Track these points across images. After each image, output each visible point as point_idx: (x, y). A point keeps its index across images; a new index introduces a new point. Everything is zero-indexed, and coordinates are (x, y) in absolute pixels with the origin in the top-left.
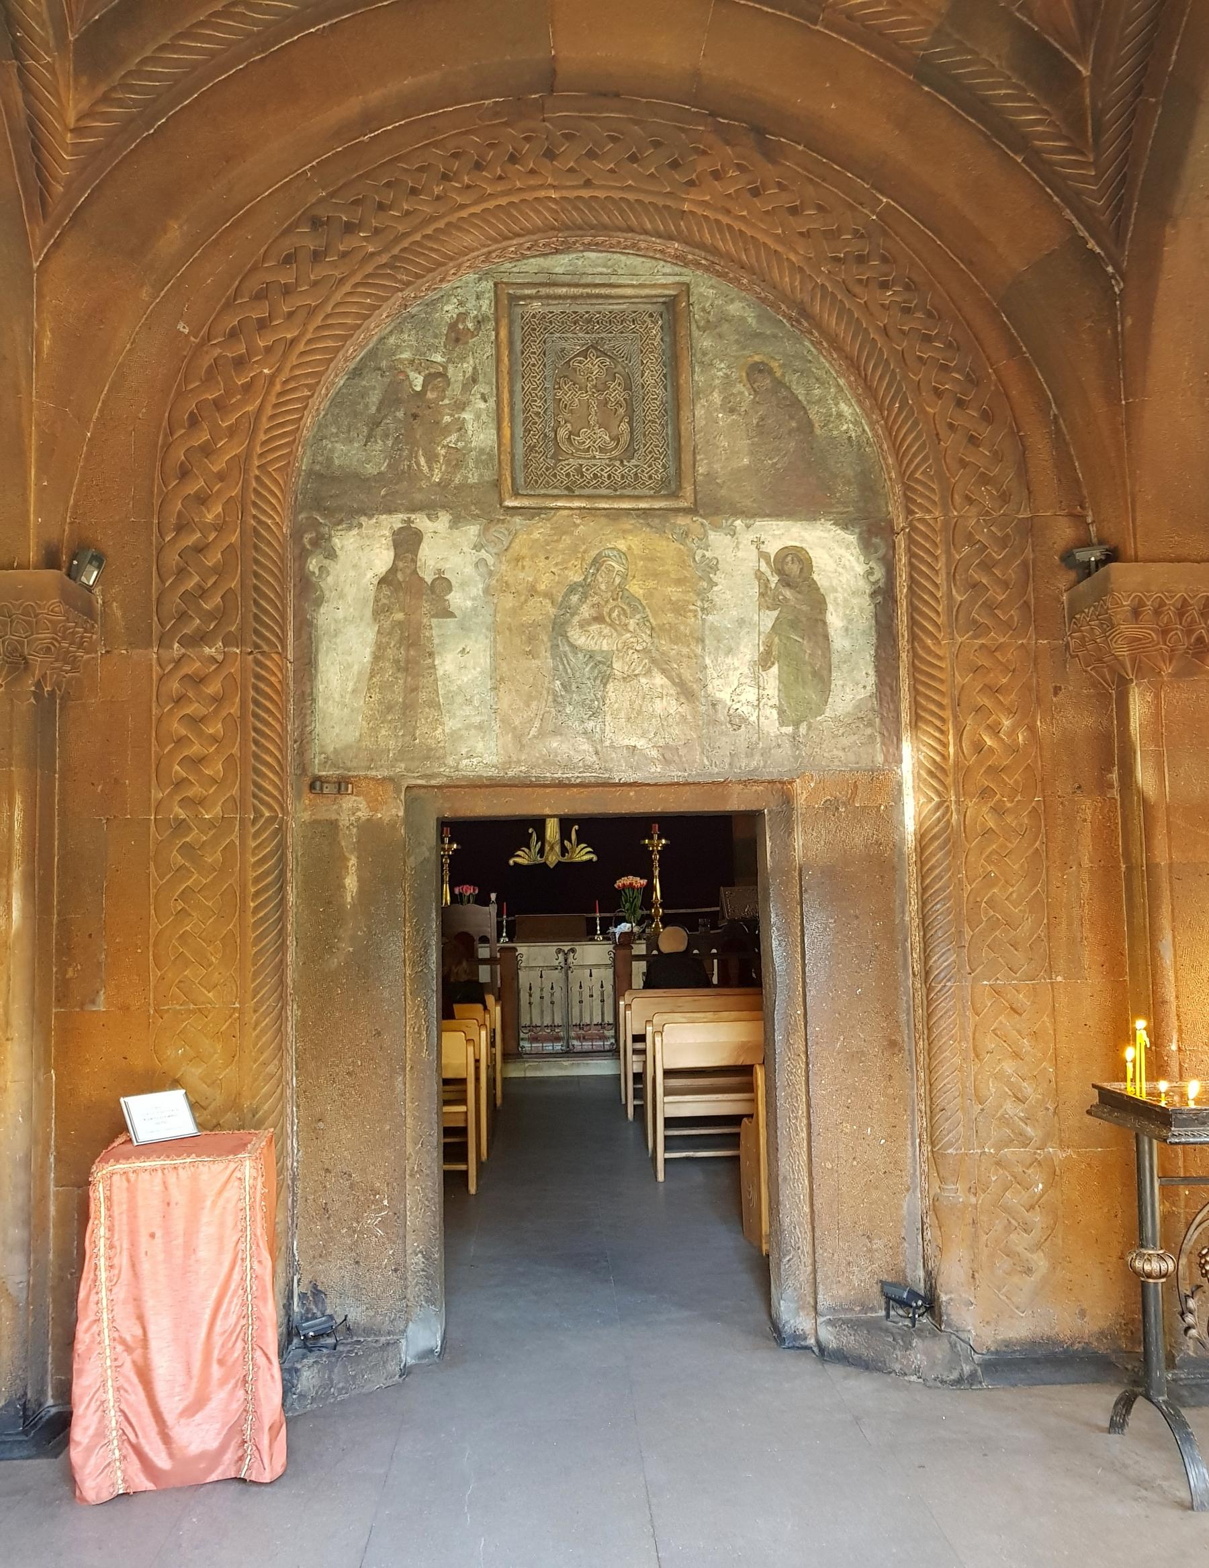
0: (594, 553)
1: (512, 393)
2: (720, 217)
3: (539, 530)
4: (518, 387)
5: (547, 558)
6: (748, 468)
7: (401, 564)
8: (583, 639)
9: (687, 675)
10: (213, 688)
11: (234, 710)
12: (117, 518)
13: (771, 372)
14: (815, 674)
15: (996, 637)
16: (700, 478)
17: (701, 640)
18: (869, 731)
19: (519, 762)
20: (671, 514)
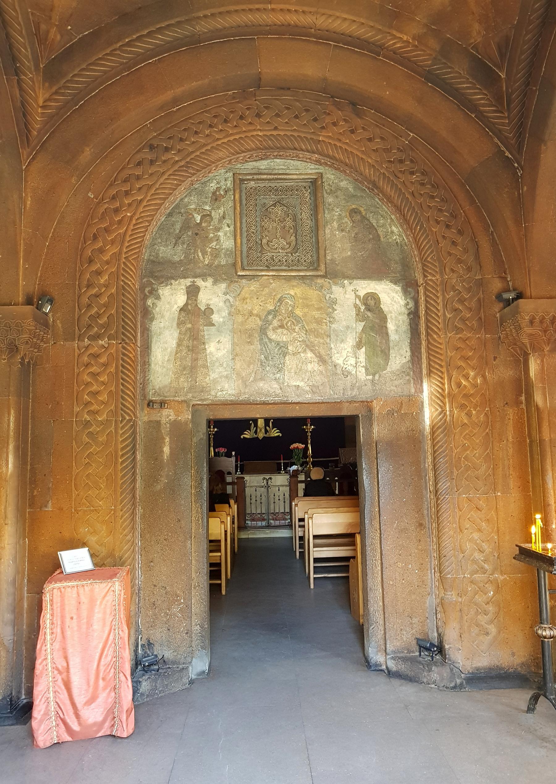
0: (279, 296)
1: (241, 223)
2: (336, 143)
3: (254, 286)
4: (244, 221)
5: (258, 298)
6: (350, 256)
7: (190, 302)
8: (274, 336)
9: (323, 352)
10: (103, 360)
11: (113, 370)
12: (60, 282)
13: (360, 212)
14: (382, 351)
15: (466, 334)
18: (408, 378)
19: (245, 393)
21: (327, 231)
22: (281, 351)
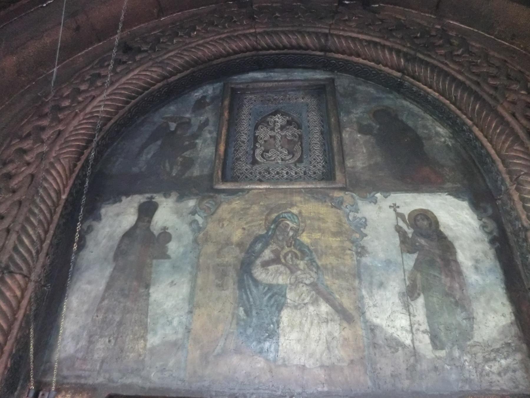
0: (274, 216)
3: (237, 204)
8: (263, 275)
17: (358, 275)
20: (328, 191)
22: (273, 300)
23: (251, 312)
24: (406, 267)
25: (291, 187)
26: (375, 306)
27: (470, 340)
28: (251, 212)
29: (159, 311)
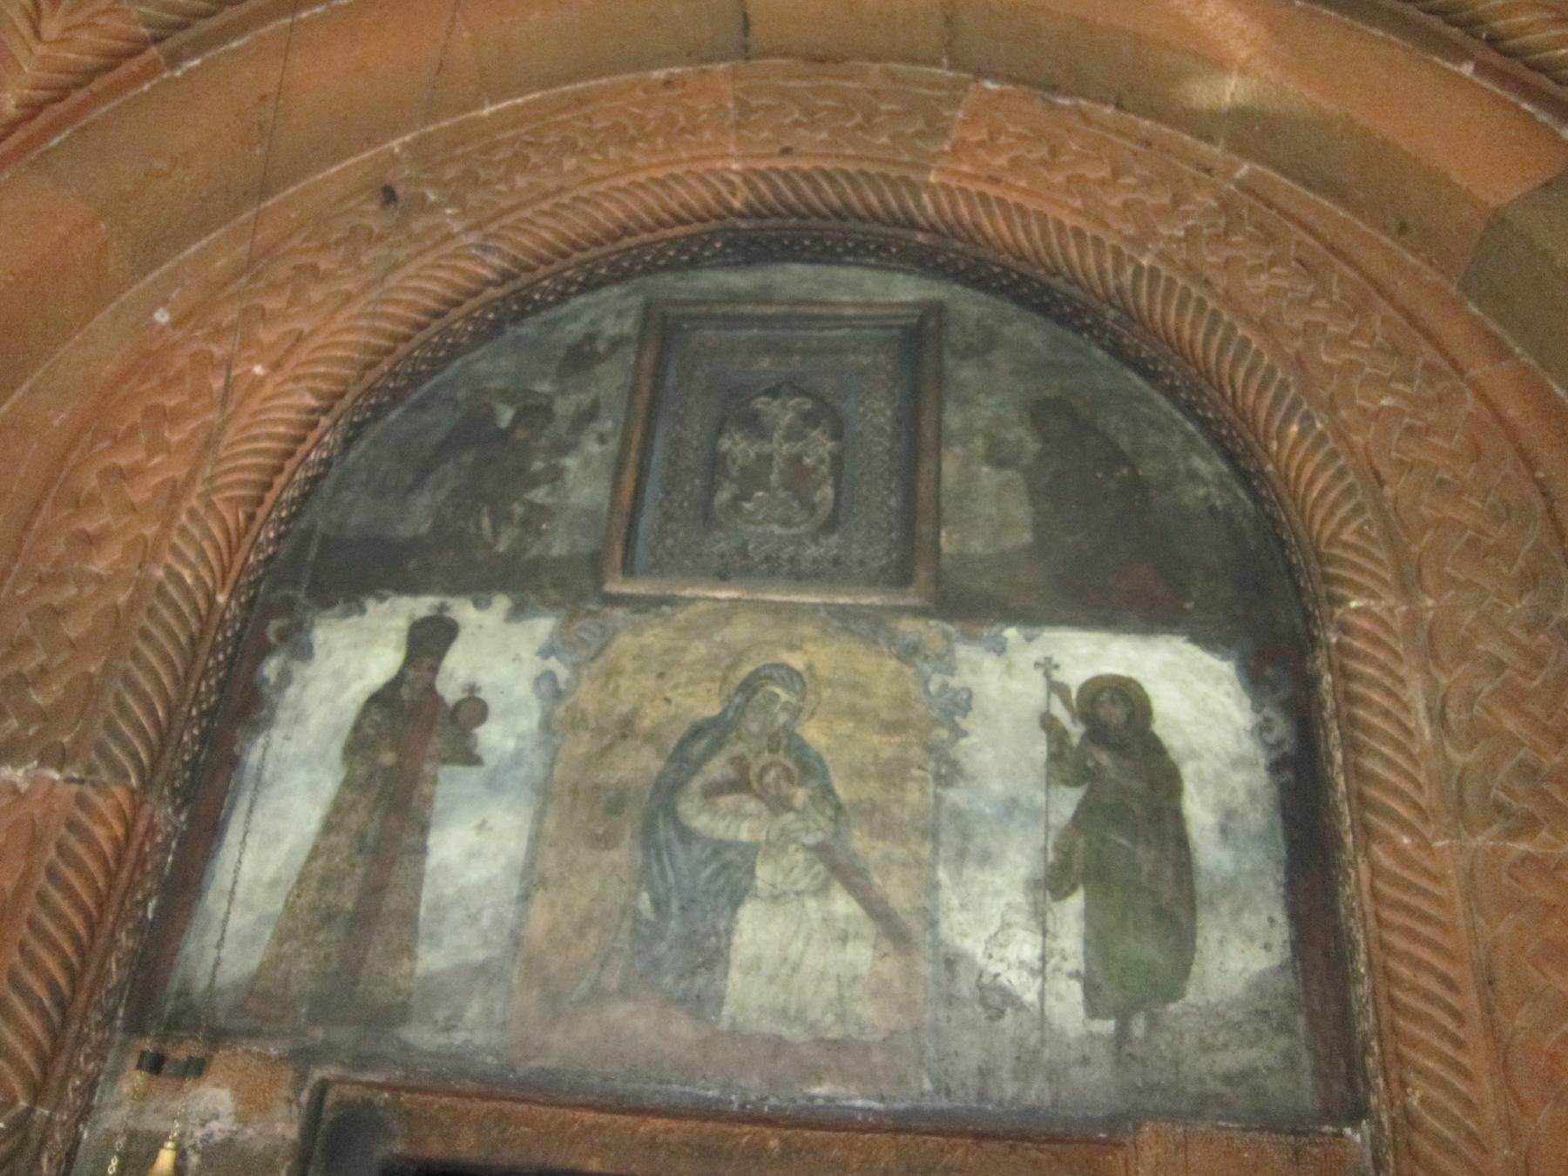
0: (746, 670)
3: (655, 636)
4: (661, 433)
7: (411, 674)
16: (945, 561)
17: (931, 833)
18: (1283, 1042)
21: (949, 467)
22: (721, 881)
23: (668, 903)
24: (1053, 820)
25: (795, 598)
26: (963, 907)
27: (1175, 999)
28: (689, 657)
29: (449, 891)
